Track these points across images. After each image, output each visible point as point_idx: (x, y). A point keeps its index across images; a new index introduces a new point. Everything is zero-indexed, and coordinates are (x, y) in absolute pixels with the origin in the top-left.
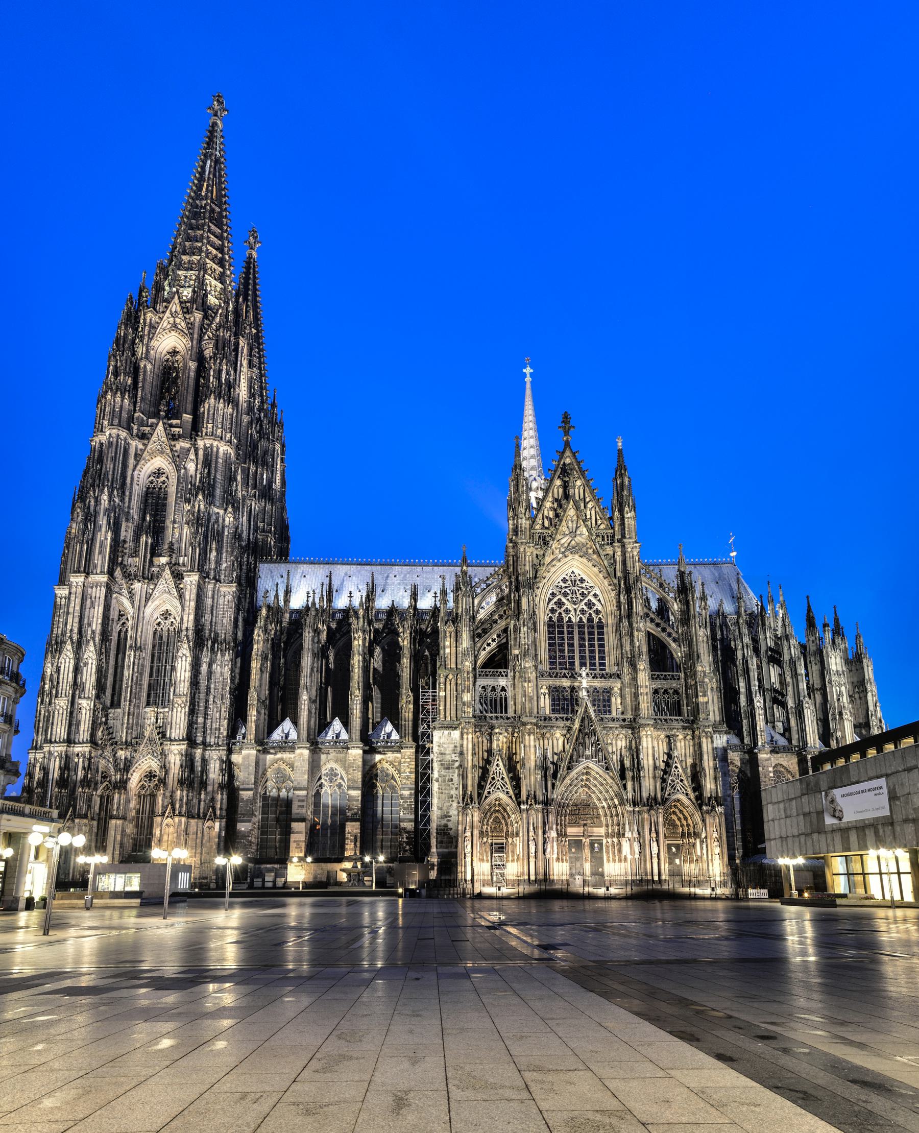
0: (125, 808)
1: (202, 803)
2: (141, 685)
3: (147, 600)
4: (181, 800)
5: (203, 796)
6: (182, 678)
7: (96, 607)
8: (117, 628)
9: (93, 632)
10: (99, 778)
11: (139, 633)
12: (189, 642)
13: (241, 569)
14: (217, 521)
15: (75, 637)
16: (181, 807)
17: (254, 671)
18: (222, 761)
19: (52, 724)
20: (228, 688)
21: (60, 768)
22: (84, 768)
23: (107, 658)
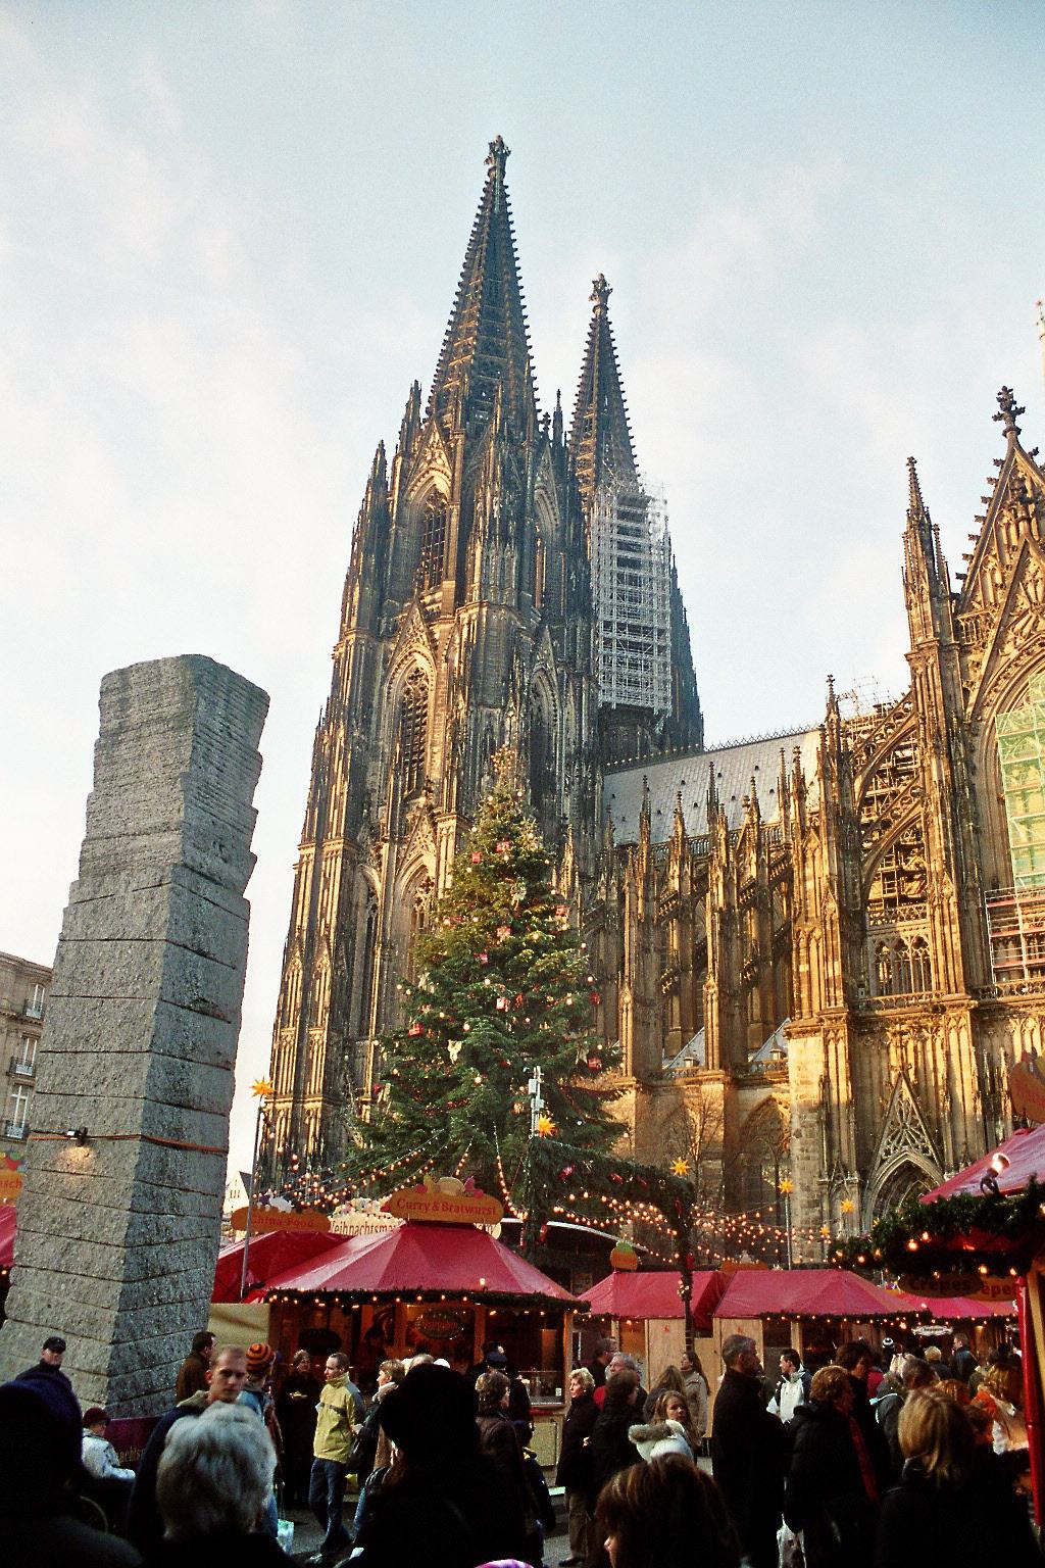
9: (327, 927)
14: (490, 729)
23: (350, 964)
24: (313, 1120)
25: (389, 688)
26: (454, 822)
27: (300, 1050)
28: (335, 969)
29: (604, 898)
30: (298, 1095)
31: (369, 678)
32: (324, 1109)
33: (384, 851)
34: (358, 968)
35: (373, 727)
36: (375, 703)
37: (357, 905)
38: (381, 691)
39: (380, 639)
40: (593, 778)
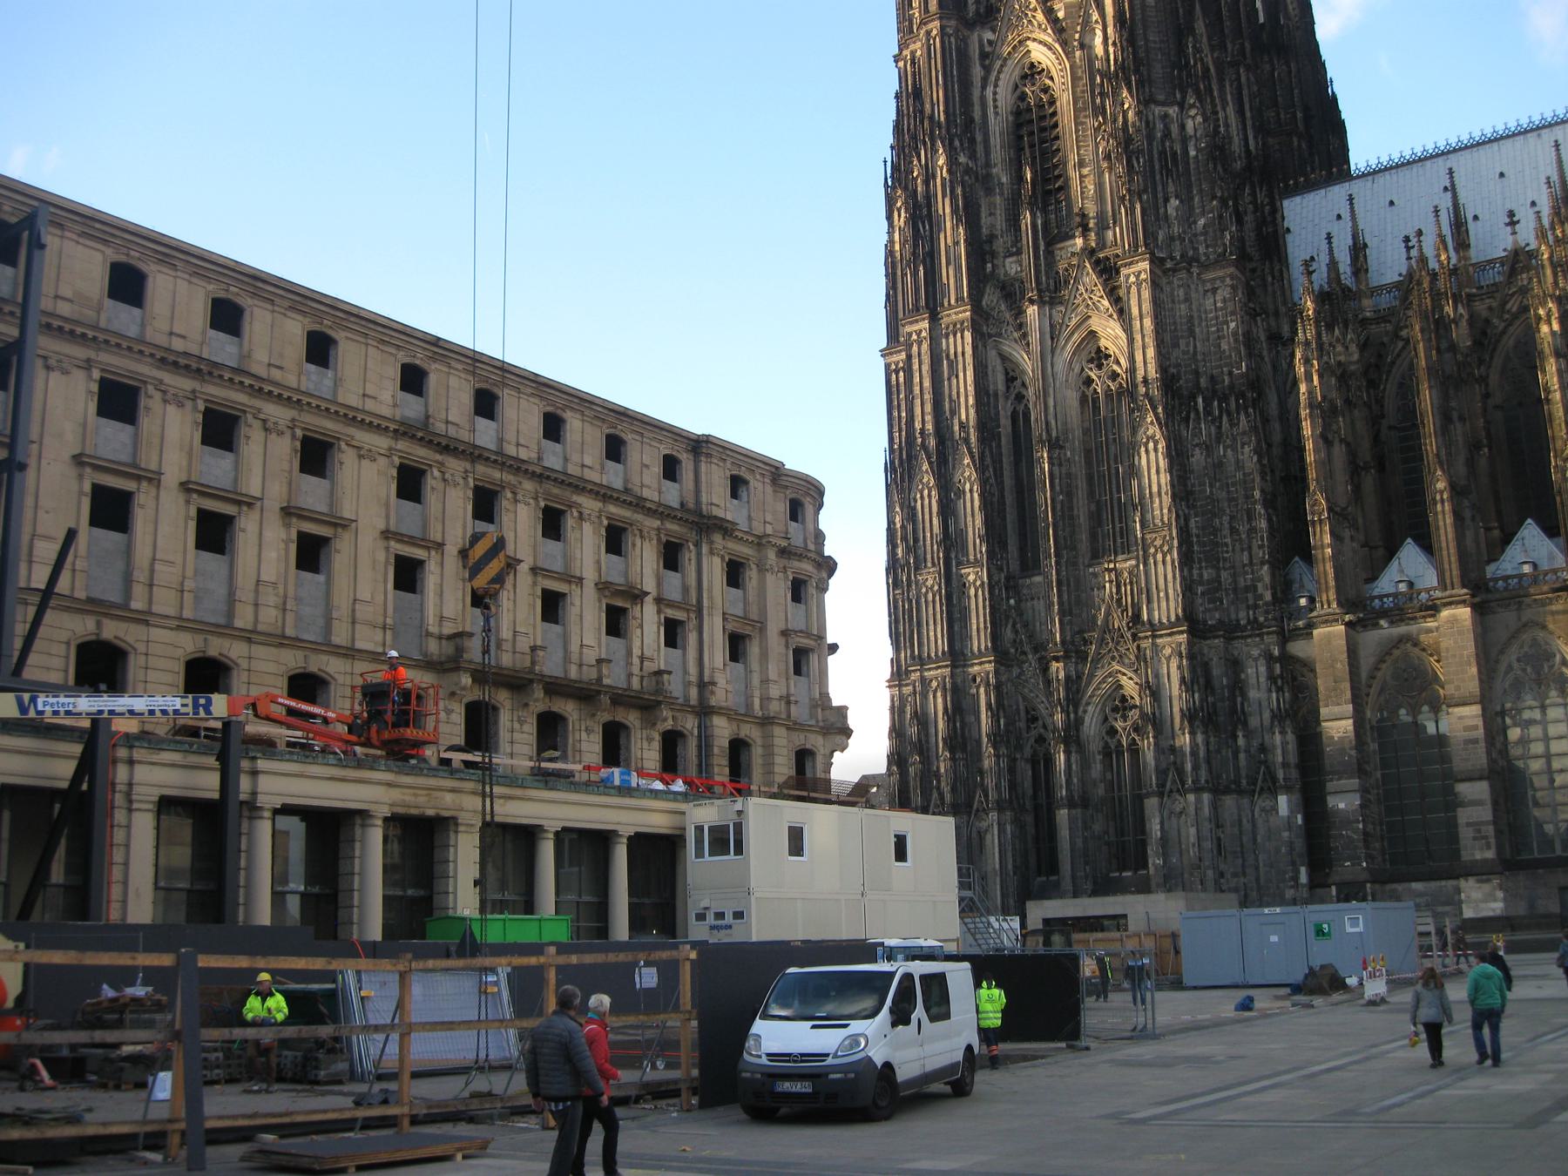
0: (1082, 782)
7: (961, 375)
8: (1005, 409)
12: (1154, 409)
14: (1167, 134)
15: (932, 442)
16: (1196, 768)
17: (1309, 445)
21: (945, 709)
22: (989, 705)
23: (999, 474)
24: (982, 690)
25: (995, 93)
26: (1145, 265)
27: (949, 597)
28: (983, 482)
29: (1342, 358)
30: (957, 655)
31: (966, 84)
32: (996, 672)
33: (1032, 311)
34: (1008, 481)
35: (980, 148)
36: (977, 114)
37: (996, 395)
38: (983, 99)
39: (970, 25)
40: (1272, 203)
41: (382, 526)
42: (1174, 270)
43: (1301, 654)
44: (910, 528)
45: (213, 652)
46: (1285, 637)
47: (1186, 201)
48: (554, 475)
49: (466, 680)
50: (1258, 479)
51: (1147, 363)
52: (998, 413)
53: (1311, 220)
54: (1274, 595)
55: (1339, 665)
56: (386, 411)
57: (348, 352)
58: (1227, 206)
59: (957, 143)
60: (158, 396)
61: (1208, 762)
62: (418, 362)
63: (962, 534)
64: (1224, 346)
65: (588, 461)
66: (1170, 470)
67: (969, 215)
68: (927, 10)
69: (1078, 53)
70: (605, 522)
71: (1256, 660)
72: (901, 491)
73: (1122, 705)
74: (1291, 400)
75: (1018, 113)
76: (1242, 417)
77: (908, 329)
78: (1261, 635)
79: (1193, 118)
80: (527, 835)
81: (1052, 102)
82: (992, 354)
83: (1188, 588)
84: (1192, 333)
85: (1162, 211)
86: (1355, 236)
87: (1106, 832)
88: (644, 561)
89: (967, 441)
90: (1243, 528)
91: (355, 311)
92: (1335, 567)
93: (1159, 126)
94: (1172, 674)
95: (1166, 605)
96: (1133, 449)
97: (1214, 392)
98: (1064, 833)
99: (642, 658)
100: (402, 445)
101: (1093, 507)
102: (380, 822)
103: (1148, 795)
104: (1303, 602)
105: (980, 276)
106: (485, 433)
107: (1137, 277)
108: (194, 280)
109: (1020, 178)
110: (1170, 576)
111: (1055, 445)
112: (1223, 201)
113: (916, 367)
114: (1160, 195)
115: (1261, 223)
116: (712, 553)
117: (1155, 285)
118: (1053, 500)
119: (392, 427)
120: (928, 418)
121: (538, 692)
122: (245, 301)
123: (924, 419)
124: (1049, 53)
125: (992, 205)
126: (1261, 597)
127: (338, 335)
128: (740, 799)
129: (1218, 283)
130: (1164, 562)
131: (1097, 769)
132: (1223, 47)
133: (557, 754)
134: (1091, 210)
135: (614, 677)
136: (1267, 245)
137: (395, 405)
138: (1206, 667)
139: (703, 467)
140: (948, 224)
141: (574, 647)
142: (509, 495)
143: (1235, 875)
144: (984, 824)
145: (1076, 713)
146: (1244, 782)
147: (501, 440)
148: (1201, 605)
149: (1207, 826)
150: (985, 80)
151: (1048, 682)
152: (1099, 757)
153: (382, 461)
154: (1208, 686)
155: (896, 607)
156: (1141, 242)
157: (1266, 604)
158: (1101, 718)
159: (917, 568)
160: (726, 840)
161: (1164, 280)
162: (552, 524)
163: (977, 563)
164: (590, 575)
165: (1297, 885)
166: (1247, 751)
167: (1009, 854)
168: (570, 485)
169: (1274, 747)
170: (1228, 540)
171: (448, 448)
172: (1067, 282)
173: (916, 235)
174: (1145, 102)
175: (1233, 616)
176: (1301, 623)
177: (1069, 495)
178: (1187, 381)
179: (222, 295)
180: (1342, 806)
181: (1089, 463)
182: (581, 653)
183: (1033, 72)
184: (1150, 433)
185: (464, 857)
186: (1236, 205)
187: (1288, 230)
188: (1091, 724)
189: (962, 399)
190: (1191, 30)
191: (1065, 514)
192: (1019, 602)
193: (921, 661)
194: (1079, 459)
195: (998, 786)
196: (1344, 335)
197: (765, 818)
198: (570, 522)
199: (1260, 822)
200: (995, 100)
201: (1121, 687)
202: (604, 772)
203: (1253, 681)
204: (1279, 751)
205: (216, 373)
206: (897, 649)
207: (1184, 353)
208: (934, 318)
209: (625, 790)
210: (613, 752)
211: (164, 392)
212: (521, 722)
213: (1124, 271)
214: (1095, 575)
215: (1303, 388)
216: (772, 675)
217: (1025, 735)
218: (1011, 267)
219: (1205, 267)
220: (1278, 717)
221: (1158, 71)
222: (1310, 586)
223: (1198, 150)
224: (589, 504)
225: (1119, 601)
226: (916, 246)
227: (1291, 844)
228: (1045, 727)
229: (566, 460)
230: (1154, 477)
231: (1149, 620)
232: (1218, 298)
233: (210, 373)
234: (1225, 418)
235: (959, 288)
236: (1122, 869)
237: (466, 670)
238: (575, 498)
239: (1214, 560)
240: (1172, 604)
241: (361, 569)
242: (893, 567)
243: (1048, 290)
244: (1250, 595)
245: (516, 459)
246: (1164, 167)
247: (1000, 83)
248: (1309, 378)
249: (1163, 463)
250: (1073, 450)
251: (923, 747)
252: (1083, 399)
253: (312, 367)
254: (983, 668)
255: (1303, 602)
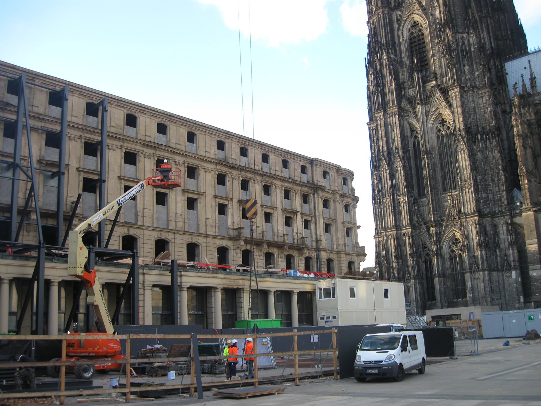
0: (443, 268)
1: (499, 258)
2: (436, 178)
3: (427, 116)
4: (482, 258)
5: (498, 253)
6: (464, 167)
7: (395, 130)
8: (411, 141)
9: (396, 148)
10: (421, 249)
11: (427, 141)
12: (463, 139)
13: (490, 72)
14: (463, 44)
15: (386, 154)
16: (483, 263)
17: (518, 149)
18: (507, 224)
19: (384, 216)
20: (500, 167)
22: (409, 243)
23: (410, 164)
24: (407, 238)
25: (402, 33)
26: (458, 90)
27: (394, 207)
28: (404, 167)
29: (529, 118)
30: (398, 227)
31: (392, 30)
32: (412, 232)
33: (419, 108)
34: (413, 166)
35: (398, 52)
36: (396, 40)
37: (407, 137)
39: (392, 10)
40: (501, 65)
41: (213, 194)
42: (468, 91)
43: (518, 222)
44: (380, 183)
45: (163, 237)
46: (512, 216)
47: (471, 66)
48: (266, 174)
49: (242, 243)
50: (500, 162)
51: (460, 123)
52: (408, 143)
53: (515, 70)
54: (508, 202)
55: (532, 226)
56: (213, 156)
57: (200, 138)
58: (486, 68)
59: (390, 51)
60: (142, 156)
61: (487, 260)
62: (222, 140)
63: (398, 185)
64: (487, 116)
65: (277, 169)
66: (470, 160)
67: (395, 75)
68: (377, 6)
69: (431, 17)
70: (284, 189)
71: (502, 224)
72: (376, 171)
73: (456, 242)
74: (511, 133)
75: (410, 39)
76: (494, 140)
77: (376, 116)
78: (504, 216)
79: (472, 37)
80: (265, 293)
81: (423, 34)
82: (406, 123)
83: (477, 201)
84: (475, 112)
85: (463, 70)
86: (531, 75)
87: (452, 286)
88: (297, 201)
89: (398, 153)
90: (496, 179)
91: (202, 124)
92: (529, 191)
93: (461, 41)
94: (473, 231)
95: (470, 207)
96: (456, 153)
97: (484, 132)
98: (437, 286)
99: (297, 233)
100: (218, 167)
101: (443, 174)
102: (220, 290)
103: (466, 273)
104: (518, 204)
105: (400, 97)
106: (243, 162)
107: (455, 93)
108: (152, 118)
109: (413, 62)
110: (471, 197)
111: (429, 153)
112: (484, 66)
113: (379, 128)
114: (462, 65)
115: (497, 72)
116: (318, 197)
117: (461, 96)
118: (429, 172)
119: (215, 161)
120: (385, 146)
121: (265, 246)
122: (167, 123)
123: (383, 146)
124: (421, 18)
125: (403, 71)
126: (503, 203)
127: (196, 132)
128: (334, 279)
129: (484, 94)
130: (469, 192)
131: (448, 264)
132: (481, 11)
133: (272, 266)
134: (438, 71)
135: (289, 240)
136: (499, 80)
137: (215, 154)
138: (485, 227)
139: (314, 169)
140: (388, 79)
141: (276, 231)
142: (253, 182)
143: (498, 299)
144: (409, 284)
145: (440, 245)
146: (500, 267)
147: (249, 164)
148: (482, 206)
149: (487, 283)
150: (399, 29)
151: (430, 235)
152: (448, 260)
153: (213, 173)
154: (486, 234)
155: (376, 211)
156: (456, 82)
157: (505, 205)
158: (448, 247)
159: (383, 197)
160: (329, 293)
161: (465, 94)
162: (267, 190)
163: (403, 195)
164: (279, 206)
165: (520, 302)
166: (500, 256)
167: (418, 294)
168: (272, 177)
169: (510, 254)
170: (491, 183)
171: (233, 167)
172: (431, 97)
173: (378, 83)
174: (455, 33)
175: (494, 210)
176: (518, 211)
177: (435, 170)
178: (474, 129)
179: (160, 122)
180: (535, 274)
181: (441, 159)
182: (278, 232)
183: (415, 24)
184: (462, 147)
185: (246, 300)
186: (488, 66)
187: (507, 74)
188: (445, 249)
189: (396, 139)
190: (470, 7)
191: (433, 177)
192: (418, 207)
193: (386, 229)
194: (437, 157)
195: (414, 271)
196: (529, 110)
197: (342, 285)
198: (272, 189)
199: (506, 281)
200: (402, 35)
201: (455, 235)
202: (288, 272)
203: (501, 232)
204: (512, 256)
205: (160, 147)
206: (377, 225)
207: (473, 119)
208: (385, 111)
209: (296, 277)
210: (289, 265)
211: (144, 154)
212: (260, 256)
213: (450, 92)
214: (445, 197)
215: (515, 129)
216: (340, 237)
217: (422, 253)
218: (411, 92)
219: (479, 89)
220: (511, 244)
221: (459, 22)
222: (521, 198)
223: (474, 48)
224: (278, 183)
225: (453, 206)
226: (377, 87)
227: (517, 288)
228: (429, 250)
229: (270, 169)
230: (464, 163)
231: (464, 213)
232: (484, 99)
233: (158, 148)
234: (488, 141)
235: (393, 100)
236: (458, 298)
237: (242, 240)
238: (274, 181)
239: (486, 191)
240: (472, 206)
241: (207, 208)
242: (374, 197)
243: (424, 99)
244: (499, 202)
245: (254, 169)
246: (463, 55)
247: (404, 29)
248: (517, 126)
249: (467, 158)
250: (435, 154)
251: (387, 258)
252: (438, 137)
253: (189, 143)
254: (407, 231)
255: (518, 204)
